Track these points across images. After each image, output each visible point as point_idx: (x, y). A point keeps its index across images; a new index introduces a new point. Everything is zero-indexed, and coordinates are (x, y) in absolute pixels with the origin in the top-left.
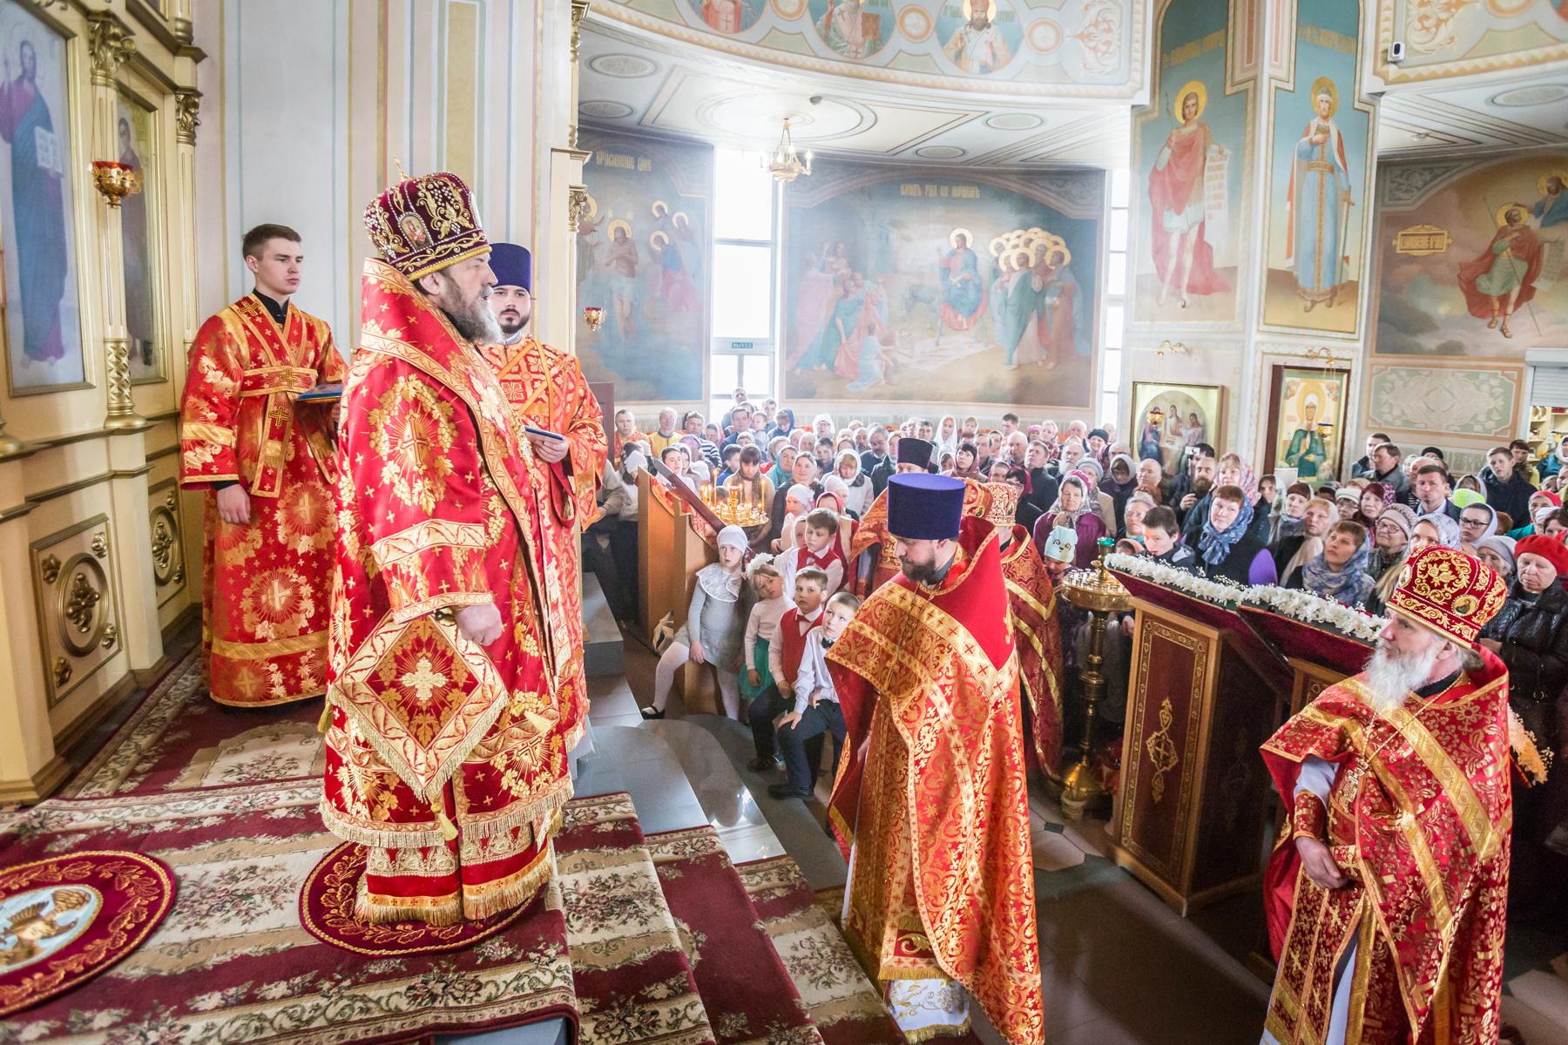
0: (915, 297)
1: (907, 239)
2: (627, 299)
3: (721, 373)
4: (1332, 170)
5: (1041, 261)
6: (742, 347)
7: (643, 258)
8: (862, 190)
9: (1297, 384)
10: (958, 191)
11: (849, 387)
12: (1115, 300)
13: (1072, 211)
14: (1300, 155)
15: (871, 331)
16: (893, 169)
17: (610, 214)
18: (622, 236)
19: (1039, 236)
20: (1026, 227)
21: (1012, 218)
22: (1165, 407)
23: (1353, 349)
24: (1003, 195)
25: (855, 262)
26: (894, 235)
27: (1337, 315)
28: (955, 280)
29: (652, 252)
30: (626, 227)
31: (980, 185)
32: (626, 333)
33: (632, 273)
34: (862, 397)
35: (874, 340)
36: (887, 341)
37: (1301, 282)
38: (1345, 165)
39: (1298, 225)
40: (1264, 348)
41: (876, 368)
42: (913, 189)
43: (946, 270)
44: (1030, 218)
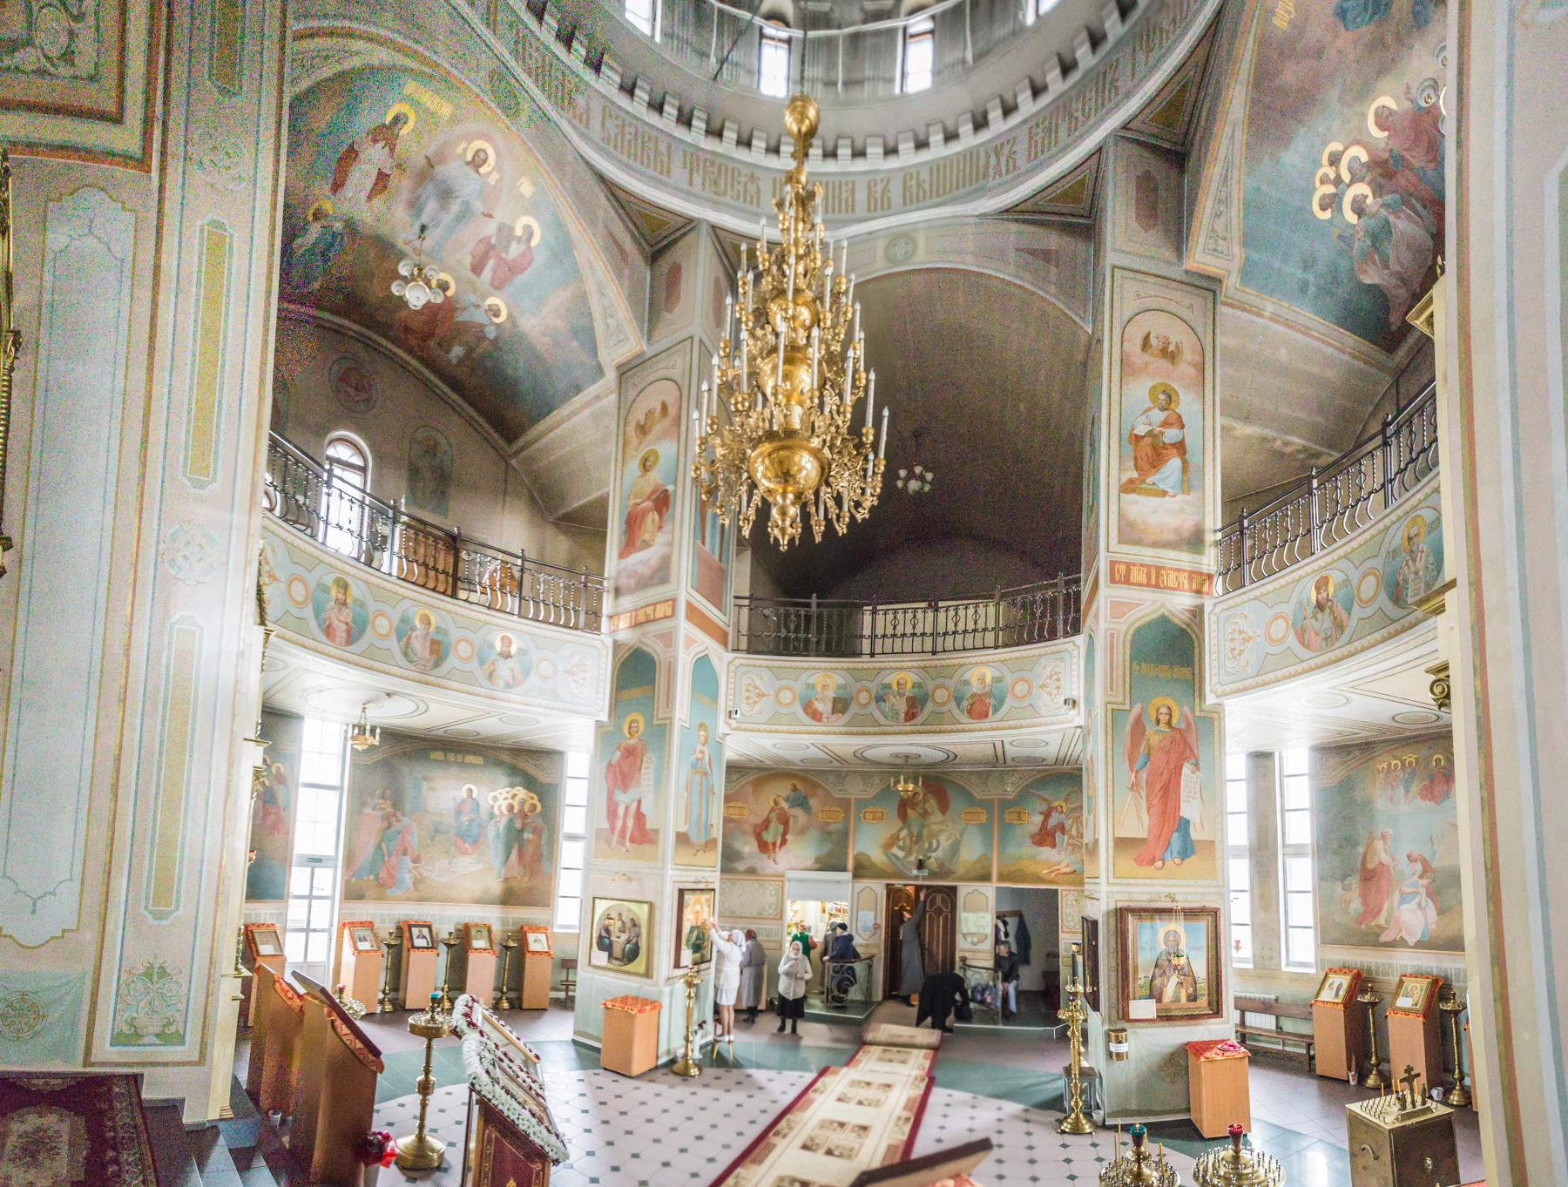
0: (437, 830)
1: (434, 789)
5: (521, 810)
8: (405, 754)
10: (470, 759)
11: (388, 891)
12: (572, 837)
13: (543, 777)
15: (405, 854)
16: (424, 740)
19: (521, 792)
20: (512, 786)
21: (505, 780)
22: (614, 914)
23: (714, 877)
24: (498, 763)
25: (397, 804)
26: (425, 786)
27: (703, 858)
28: (465, 819)
31: (484, 756)
34: (397, 899)
35: (407, 859)
36: (416, 860)
41: (408, 879)
42: (438, 755)
43: (459, 812)
44: (519, 779)
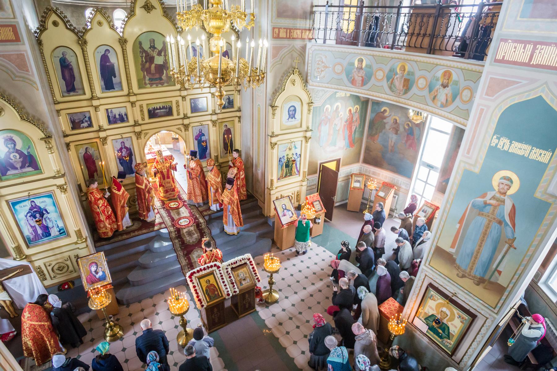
2: (394, 141)
3: (420, 172)
4: (500, 223)
6: (430, 167)
7: (401, 129)
9: (438, 299)
14: (474, 206)
17: (393, 114)
18: (396, 122)
29: (405, 128)
30: (397, 118)
32: (392, 151)
33: (396, 133)
37: (458, 262)
38: (514, 226)
39: (463, 237)
40: (427, 274)
